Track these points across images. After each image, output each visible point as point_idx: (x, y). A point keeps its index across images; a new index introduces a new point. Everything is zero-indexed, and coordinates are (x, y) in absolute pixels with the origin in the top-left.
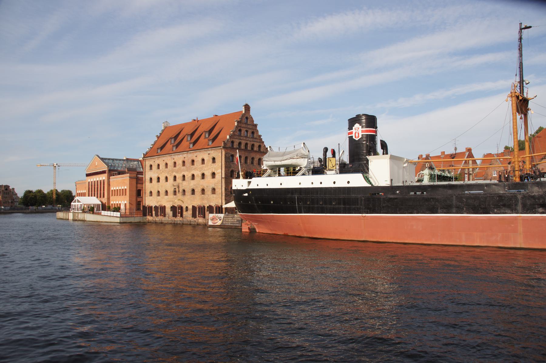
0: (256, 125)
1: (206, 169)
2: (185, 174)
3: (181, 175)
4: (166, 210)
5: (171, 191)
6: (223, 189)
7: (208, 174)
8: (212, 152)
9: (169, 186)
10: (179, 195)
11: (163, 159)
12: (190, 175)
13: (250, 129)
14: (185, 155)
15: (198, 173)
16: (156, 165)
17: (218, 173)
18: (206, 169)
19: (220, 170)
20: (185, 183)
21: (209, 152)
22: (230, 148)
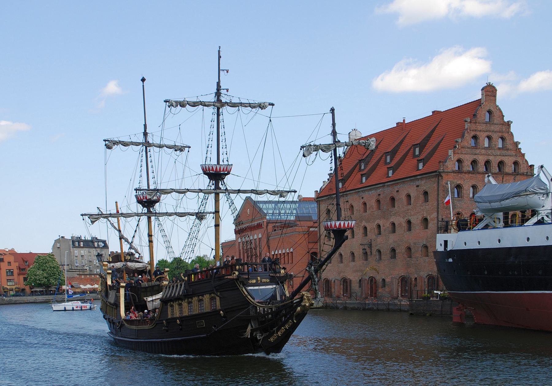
0: (508, 124)
2: (381, 223)
3: (374, 225)
4: (353, 285)
5: (358, 253)
7: (416, 220)
13: (497, 132)
15: (400, 221)
18: (412, 213)
19: (435, 215)
20: (380, 239)
22: (454, 172)
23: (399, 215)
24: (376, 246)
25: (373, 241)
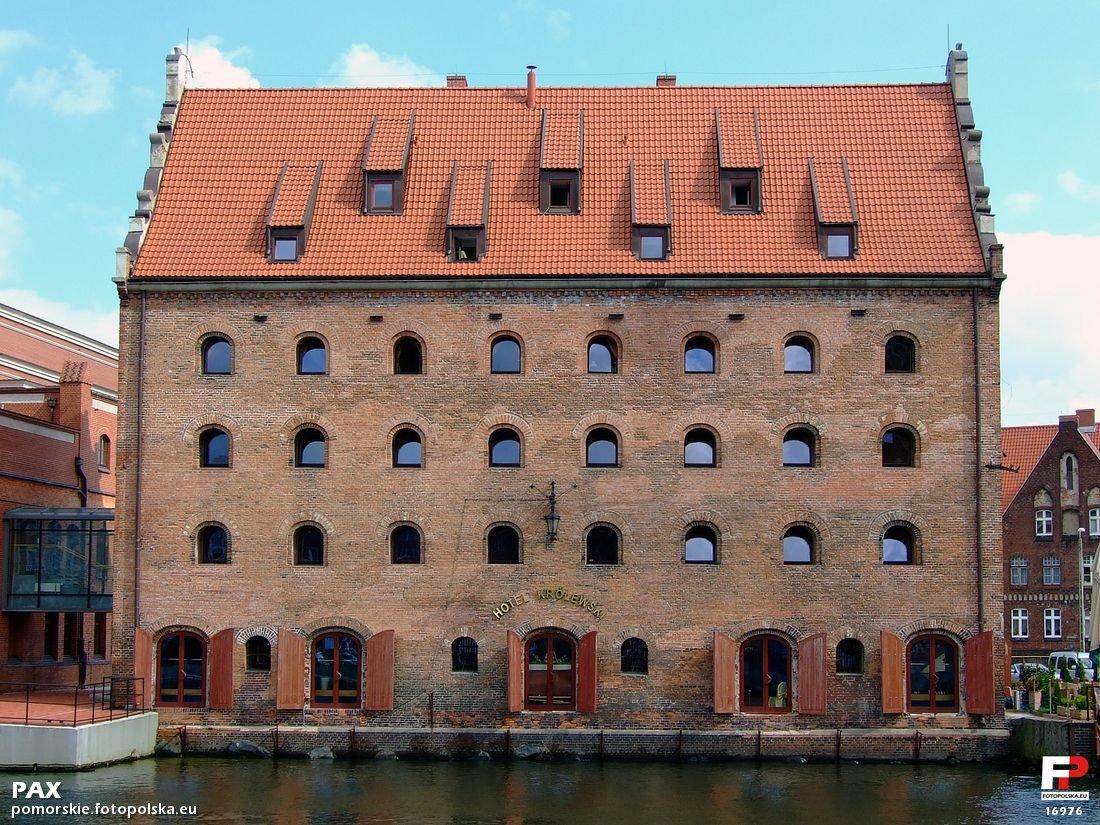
1: (826, 403)
2: (625, 423)
8: (889, 305)
9: (452, 491)
11: (377, 309)
12: (676, 430)
14: (611, 305)
18: (826, 403)
21: (857, 304)
23: (745, 405)
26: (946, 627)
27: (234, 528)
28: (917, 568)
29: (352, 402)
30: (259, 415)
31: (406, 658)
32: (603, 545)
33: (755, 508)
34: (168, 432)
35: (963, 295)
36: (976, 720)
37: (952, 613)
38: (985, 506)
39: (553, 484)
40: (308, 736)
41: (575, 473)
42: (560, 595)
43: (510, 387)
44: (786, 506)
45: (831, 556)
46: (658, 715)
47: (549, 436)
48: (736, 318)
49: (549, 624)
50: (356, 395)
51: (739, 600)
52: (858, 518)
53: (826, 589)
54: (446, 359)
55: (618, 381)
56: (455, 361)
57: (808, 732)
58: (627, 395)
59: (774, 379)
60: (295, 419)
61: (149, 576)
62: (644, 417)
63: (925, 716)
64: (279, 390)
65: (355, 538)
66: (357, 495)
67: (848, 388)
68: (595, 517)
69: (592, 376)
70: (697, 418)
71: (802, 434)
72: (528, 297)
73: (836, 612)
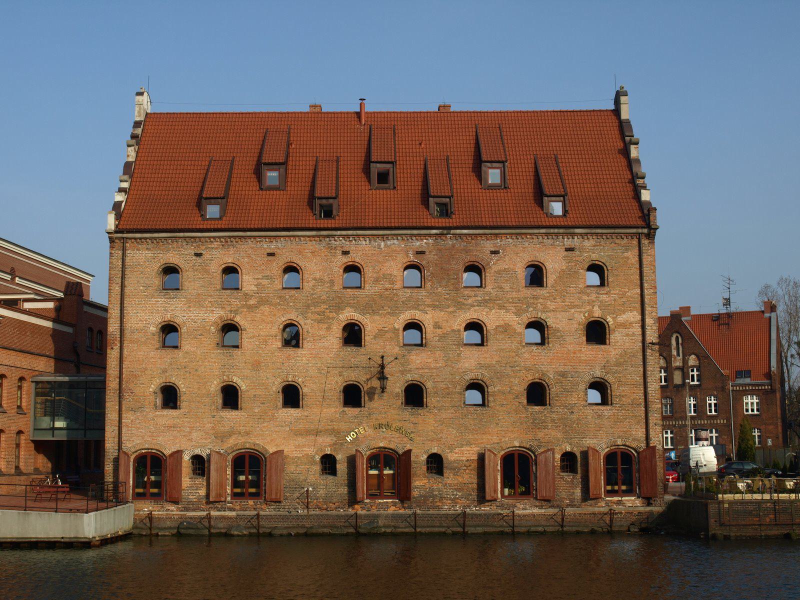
1: (551, 305)
2: (427, 319)
6: (654, 387)
8: (588, 243)
9: (321, 363)
10: (387, 406)
11: (273, 246)
14: (417, 244)
16: (216, 269)
17: (624, 325)
18: (551, 305)
19: (635, 316)
20: (418, 358)
21: (568, 242)
23: (502, 307)
24: (403, 373)
25: (387, 360)
26: (627, 443)
27: (182, 387)
28: (609, 407)
29: (256, 307)
30: (197, 314)
31: (291, 468)
32: (414, 395)
33: (509, 371)
34: (140, 325)
35: (632, 238)
36: (648, 501)
37: (632, 436)
38: (649, 368)
39: (382, 357)
40: (230, 518)
41: (397, 350)
42: (388, 426)
43: (355, 297)
44: (528, 369)
45: (556, 400)
46: (450, 502)
47: (380, 327)
48: (493, 252)
49: (382, 445)
50: (258, 302)
51: (500, 429)
52: (572, 377)
53: (553, 421)
54: (315, 279)
55: (423, 292)
56: (321, 280)
57: (543, 511)
58: (428, 301)
59: (519, 291)
60: (221, 318)
61: (128, 418)
62: (440, 315)
63: (616, 499)
64: (210, 299)
65: (258, 392)
66: (260, 365)
67: (564, 296)
68: (409, 377)
69: (406, 290)
70: (472, 315)
71: (537, 325)
72: (366, 241)
73: (559, 435)
